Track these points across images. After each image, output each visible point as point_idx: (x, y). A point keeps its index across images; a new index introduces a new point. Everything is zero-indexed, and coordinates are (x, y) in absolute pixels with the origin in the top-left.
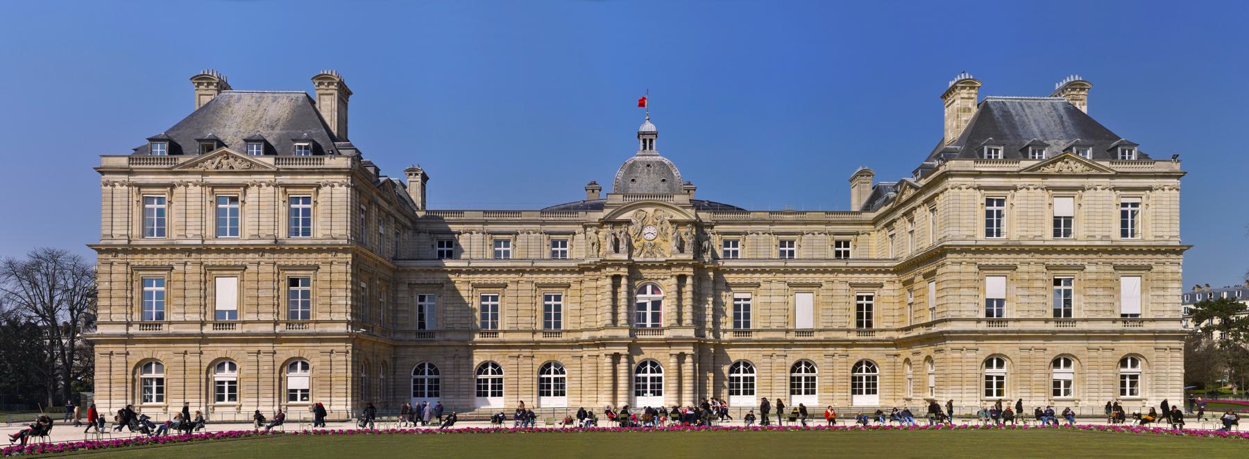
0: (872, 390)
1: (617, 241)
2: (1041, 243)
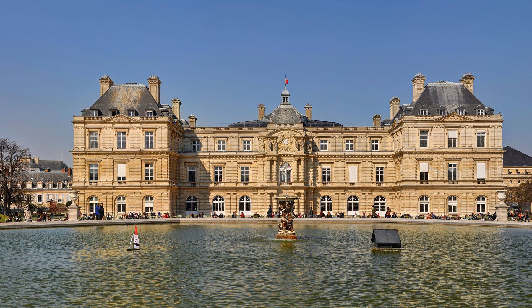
1: (272, 145)
2: (443, 150)
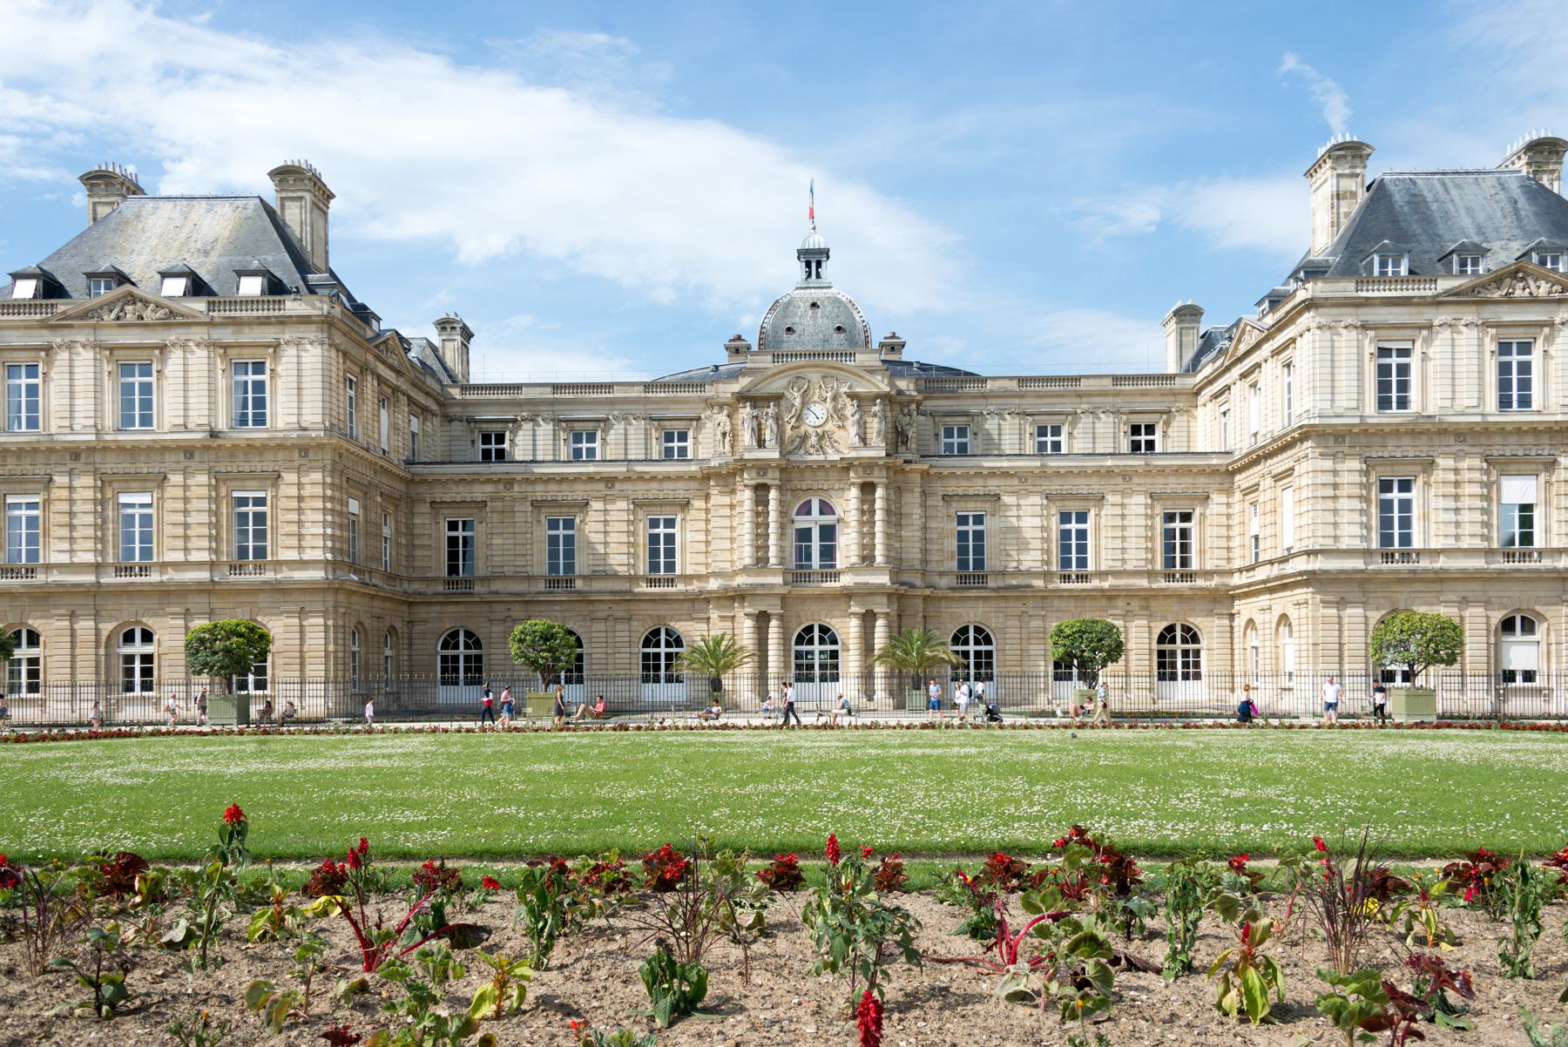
0: (1192, 672)
